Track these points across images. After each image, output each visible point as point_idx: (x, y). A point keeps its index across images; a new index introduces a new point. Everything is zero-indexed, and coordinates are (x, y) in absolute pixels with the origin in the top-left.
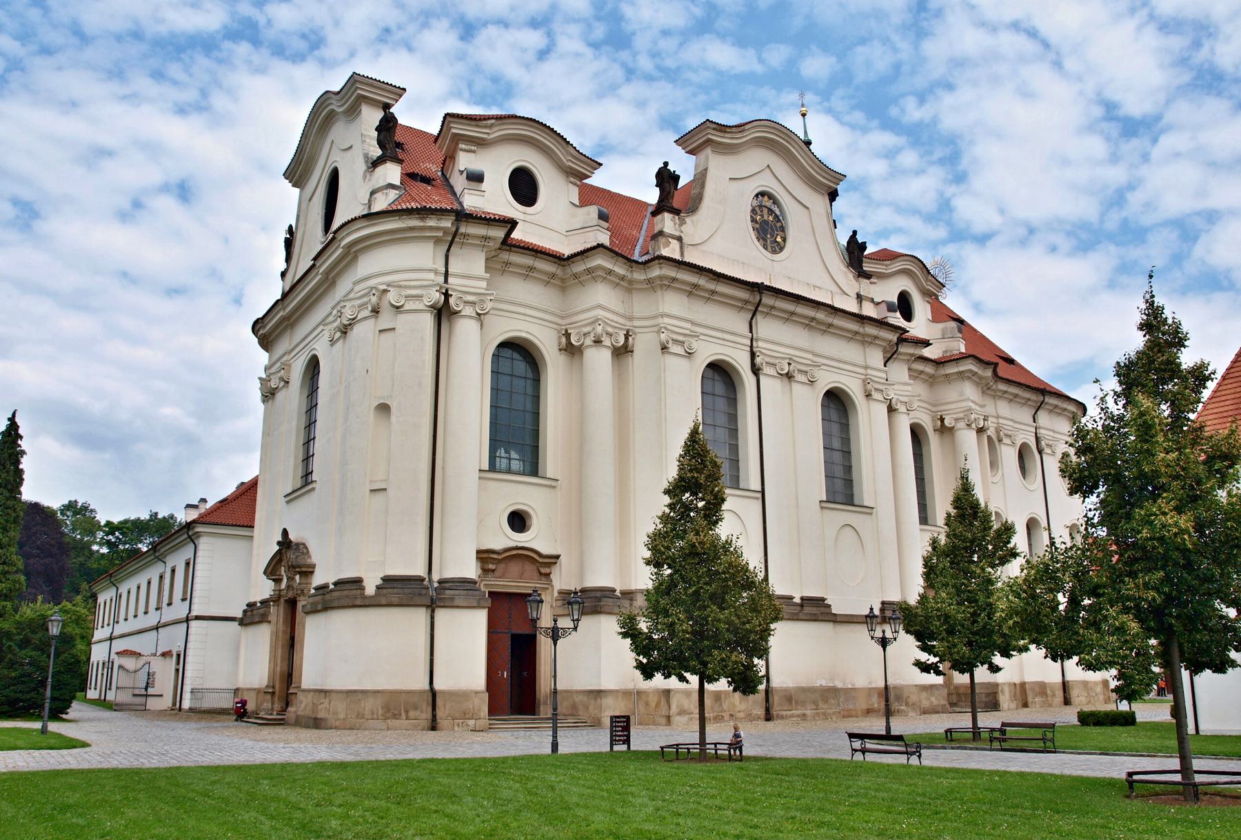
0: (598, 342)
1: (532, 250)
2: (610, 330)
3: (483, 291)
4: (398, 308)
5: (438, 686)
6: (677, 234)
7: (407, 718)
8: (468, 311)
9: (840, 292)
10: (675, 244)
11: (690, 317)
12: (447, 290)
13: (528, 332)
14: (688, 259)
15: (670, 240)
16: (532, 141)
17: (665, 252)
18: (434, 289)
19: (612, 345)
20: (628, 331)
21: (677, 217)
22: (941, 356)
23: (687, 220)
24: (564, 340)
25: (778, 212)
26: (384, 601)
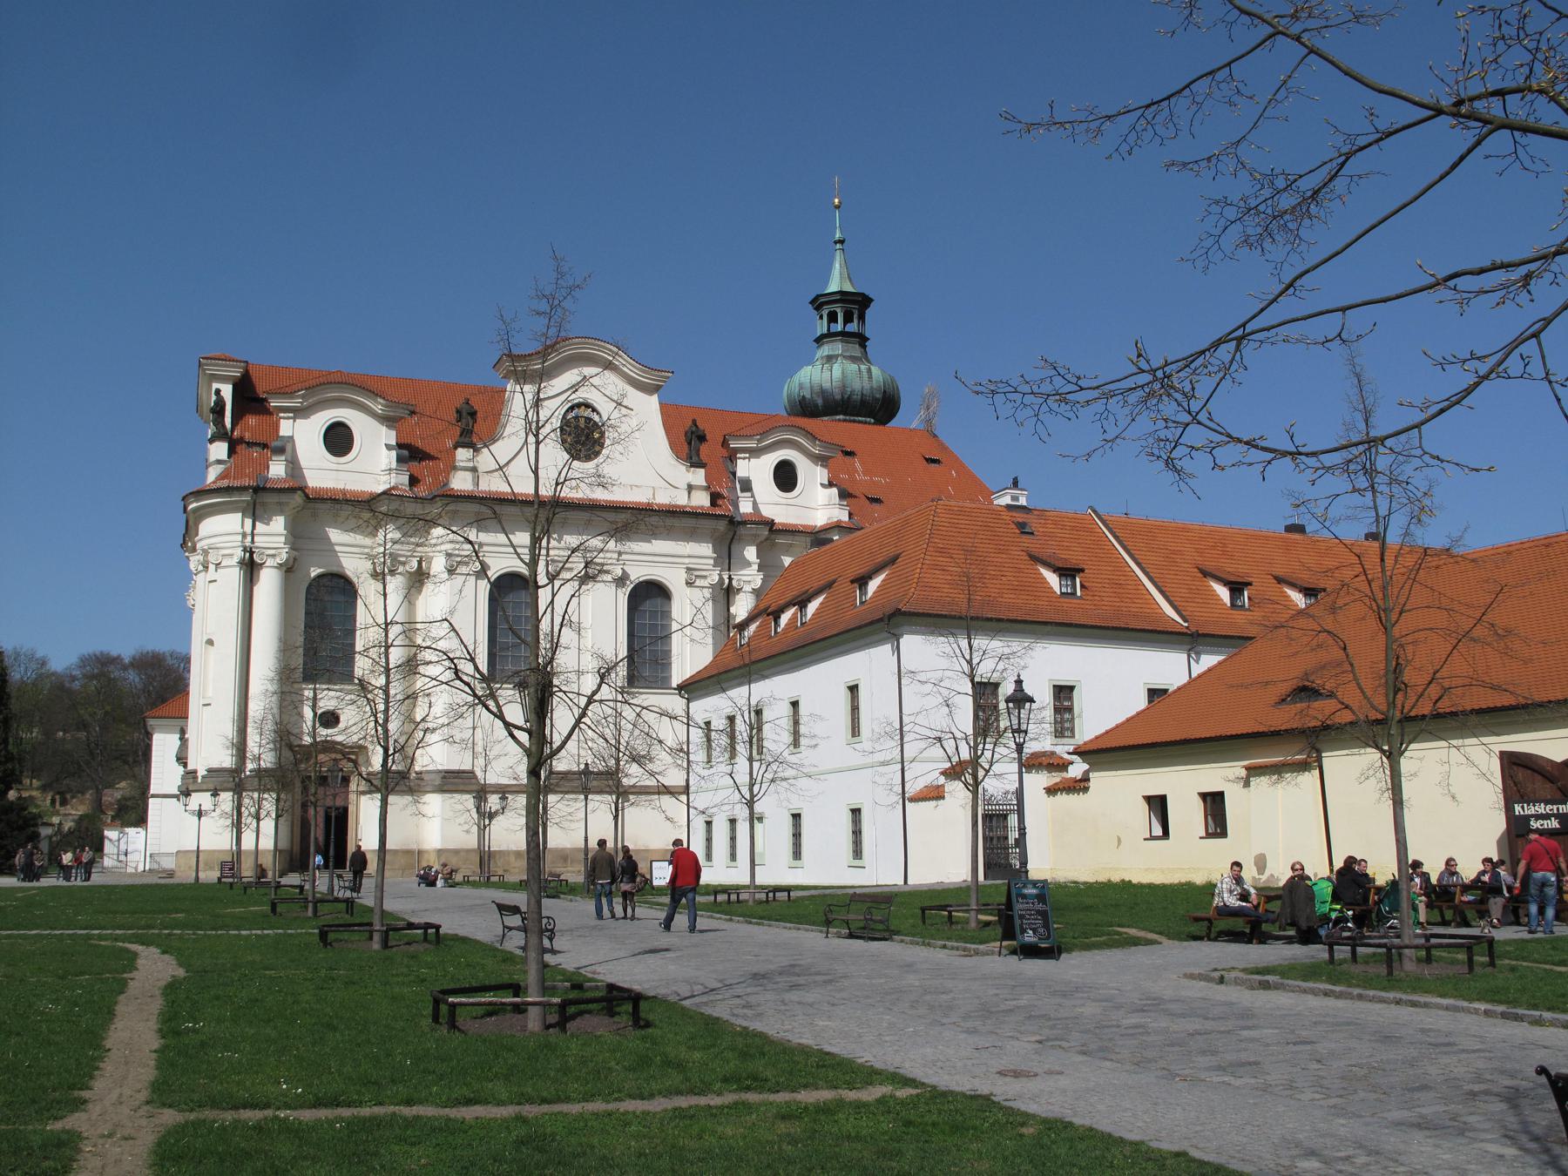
3: (282, 545)
8: (270, 562)
10: (468, 475)
20: (421, 558)
25: (596, 418)
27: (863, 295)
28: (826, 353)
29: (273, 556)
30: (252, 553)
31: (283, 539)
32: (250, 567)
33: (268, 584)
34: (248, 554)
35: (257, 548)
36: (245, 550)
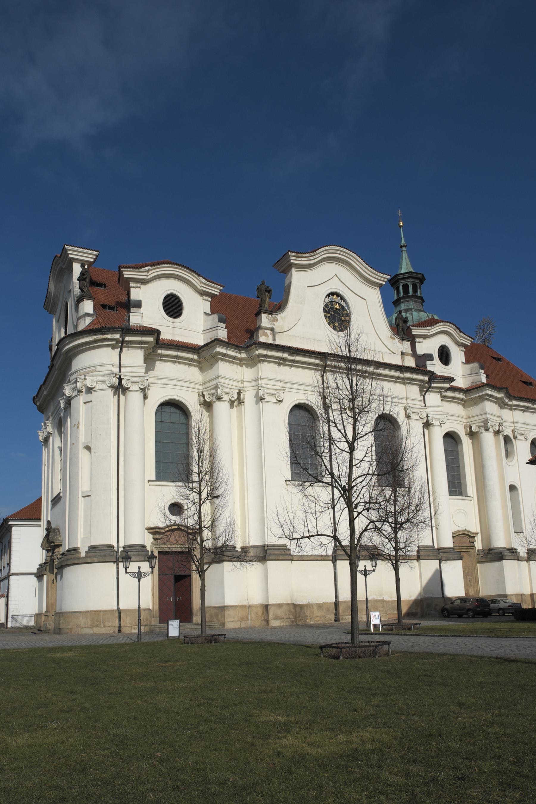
0: (219, 398)
1: (176, 346)
2: (227, 390)
3: (143, 374)
5: (121, 607)
6: (271, 326)
7: (104, 627)
9: (390, 352)
10: (268, 332)
11: (279, 377)
12: (120, 376)
13: (178, 396)
14: (278, 342)
15: (266, 331)
16: (179, 278)
17: (262, 339)
18: (112, 376)
19: (230, 400)
20: (240, 390)
21: (270, 316)
22: (470, 386)
23: (278, 317)
24: (202, 399)
25: (344, 304)
26: (89, 561)
29: (137, 382)
30: (120, 379)
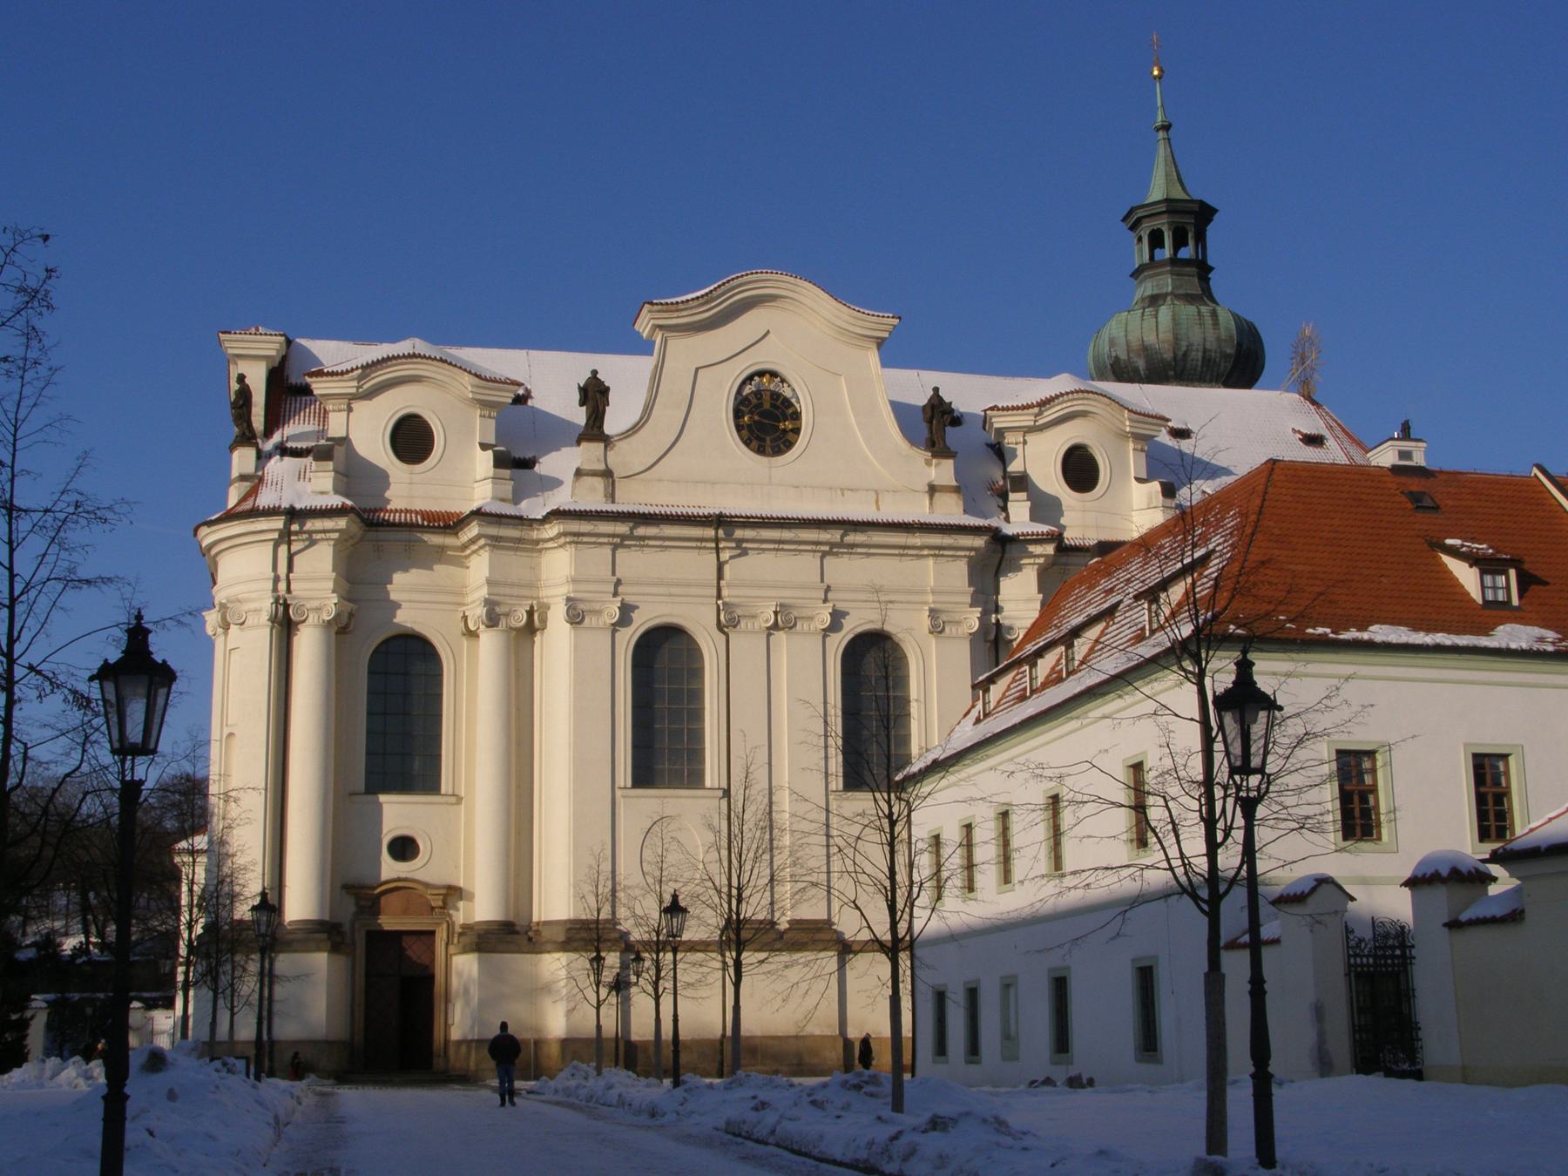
4: (243, 623)
6: (602, 467)
20: (532, 607)
25: (787, 392)
27: (1202, 203)
28: (1149, 292)
29: (318, 609)
30: (287, 606)
31: (331, 585)
32: (285, 625)
33: (308, 647)
34: (281, 609)
35: (294, 598)
36: (277, 601)
